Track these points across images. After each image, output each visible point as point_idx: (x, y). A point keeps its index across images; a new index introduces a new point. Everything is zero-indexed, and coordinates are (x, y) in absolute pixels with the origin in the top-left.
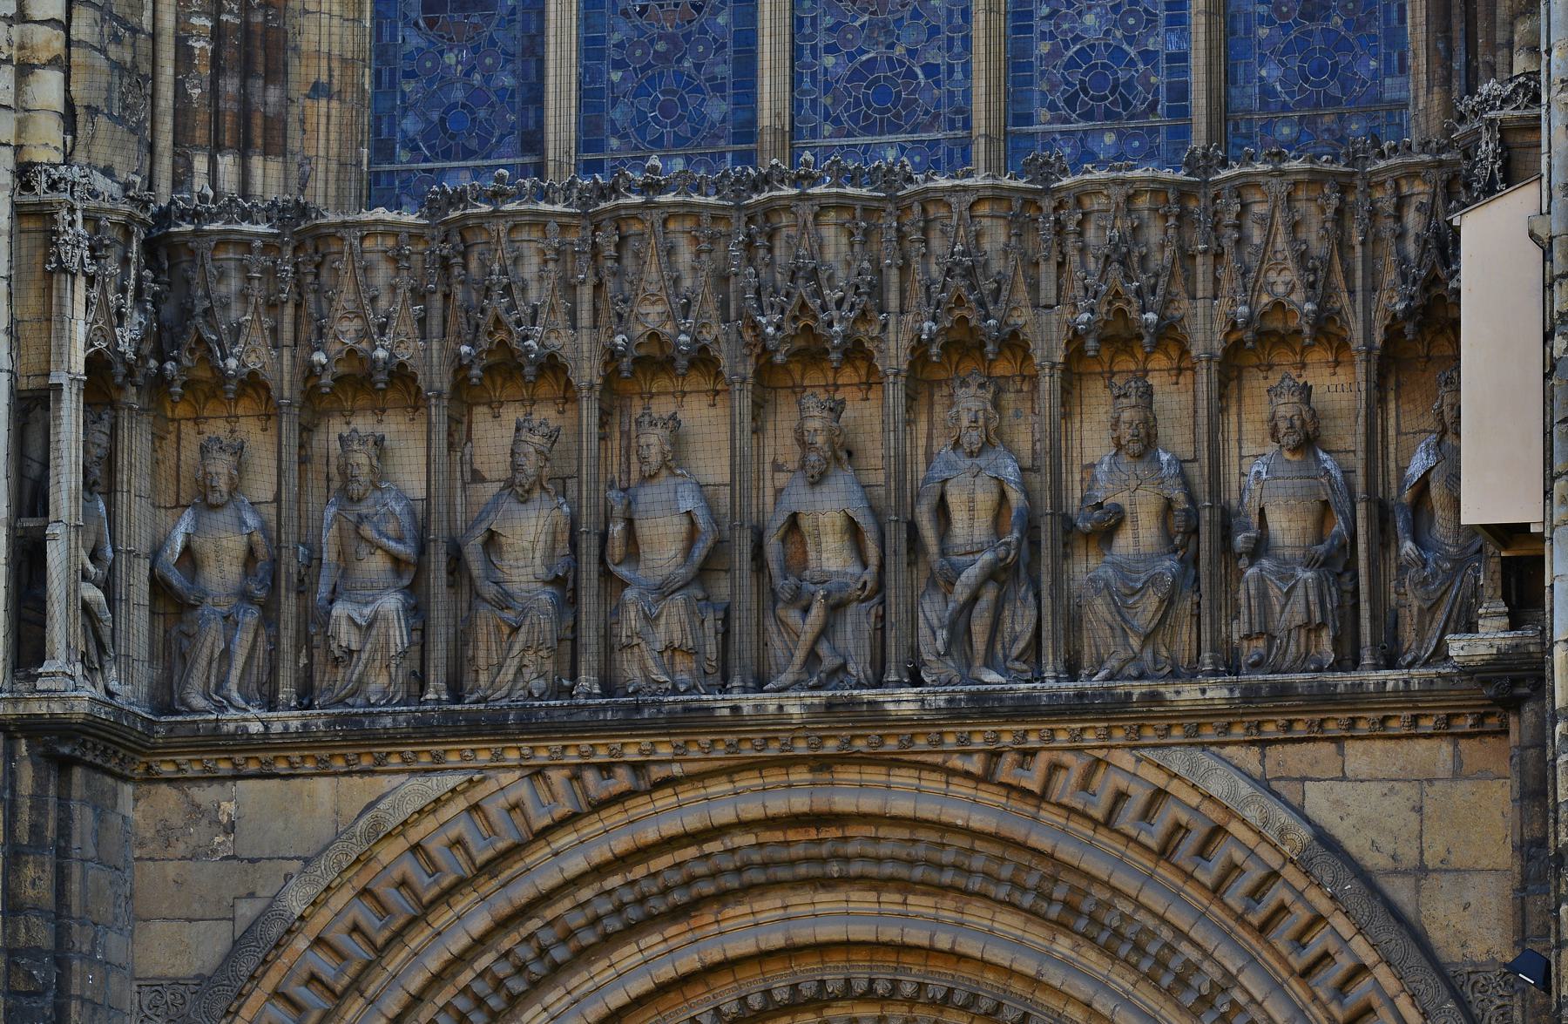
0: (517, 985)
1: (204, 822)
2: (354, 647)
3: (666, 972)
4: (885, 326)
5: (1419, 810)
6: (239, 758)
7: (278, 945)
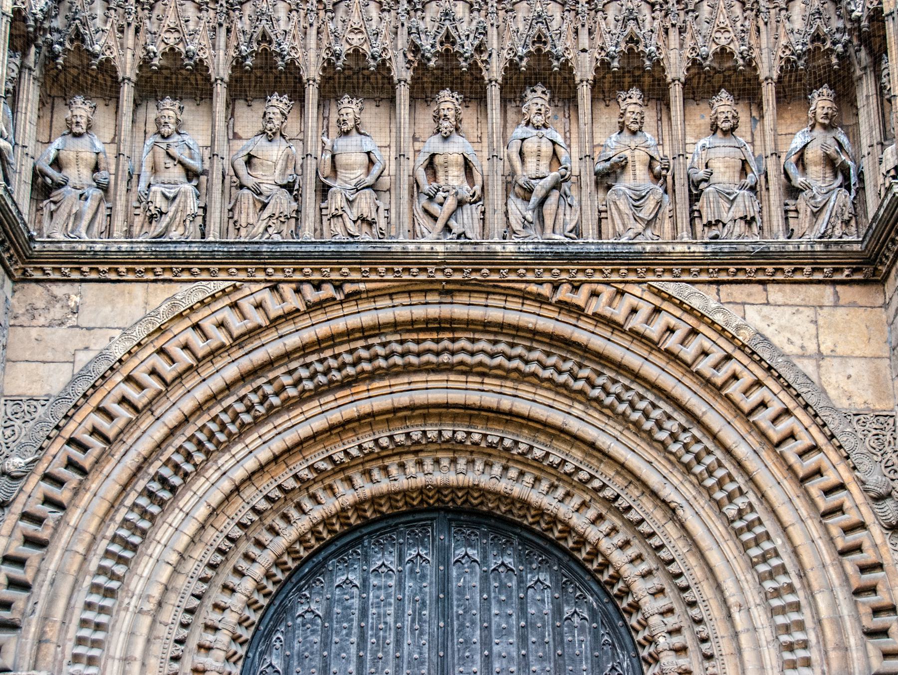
0: (247, 418)
1: (58, 306)
2: (164, 210)
3: (335, 417)
4: (490, 55)
5: (815, 322)
6: (85, 268)
7: (103, 377)
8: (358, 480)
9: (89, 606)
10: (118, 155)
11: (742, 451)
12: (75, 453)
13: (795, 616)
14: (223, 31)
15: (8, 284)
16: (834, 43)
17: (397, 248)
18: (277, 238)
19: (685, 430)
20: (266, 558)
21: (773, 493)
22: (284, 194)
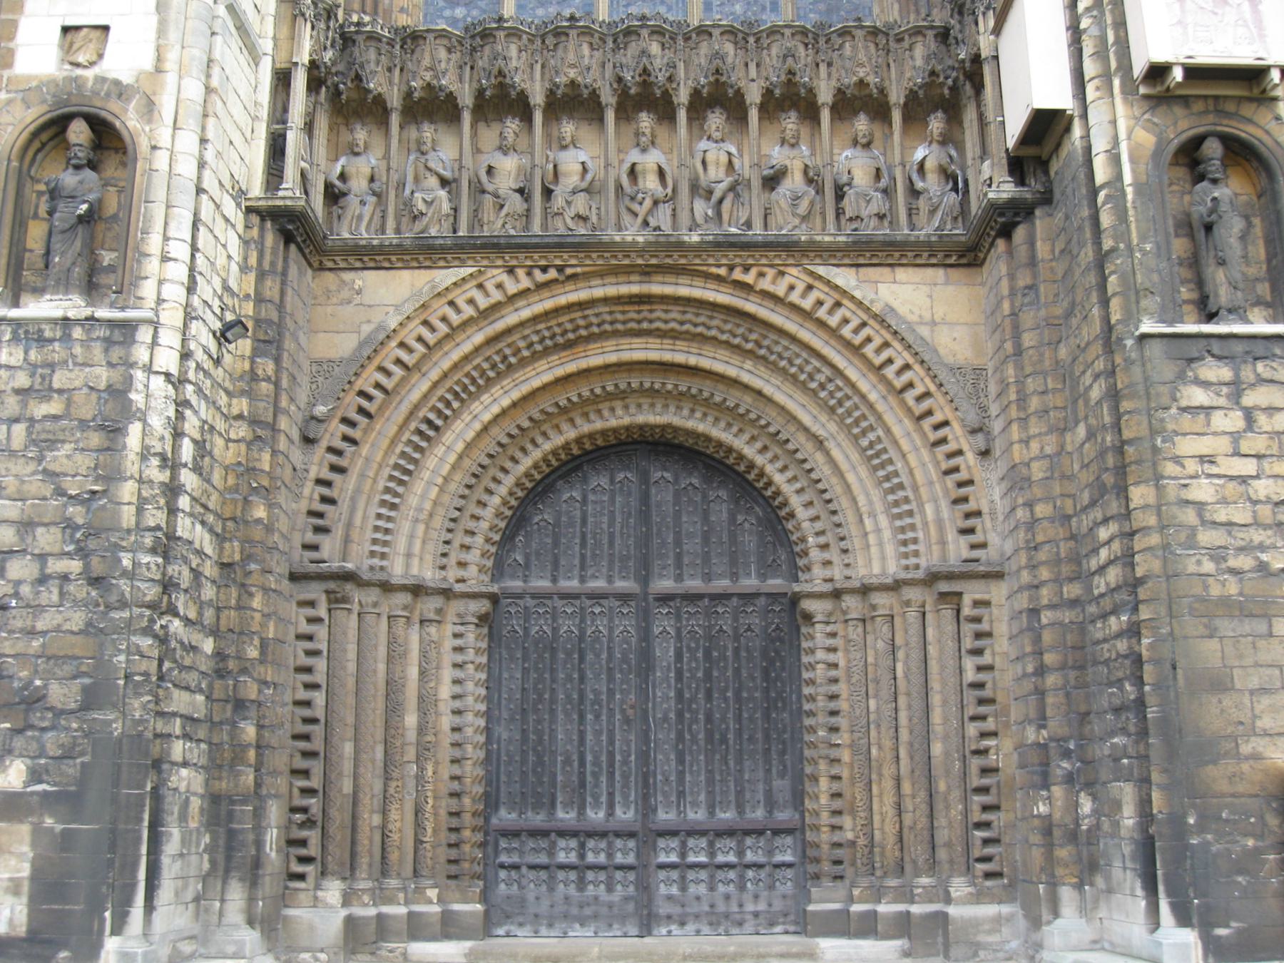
0: (491, 374)
6: (366, 259)
7: (382, 343)
8: (579, 421)
9: (379, 516)
10: (388, 169)
11: (873, 397)
12: (365, 404)
13: (908, 521)
14: (468, 68)
15: (310, 272)
16: (946, 78)
17: (606, 239)
18: (512, 232)
19: (830, 380)
20: (509, 481)
21: (897, 430)
22: (517, 195)
